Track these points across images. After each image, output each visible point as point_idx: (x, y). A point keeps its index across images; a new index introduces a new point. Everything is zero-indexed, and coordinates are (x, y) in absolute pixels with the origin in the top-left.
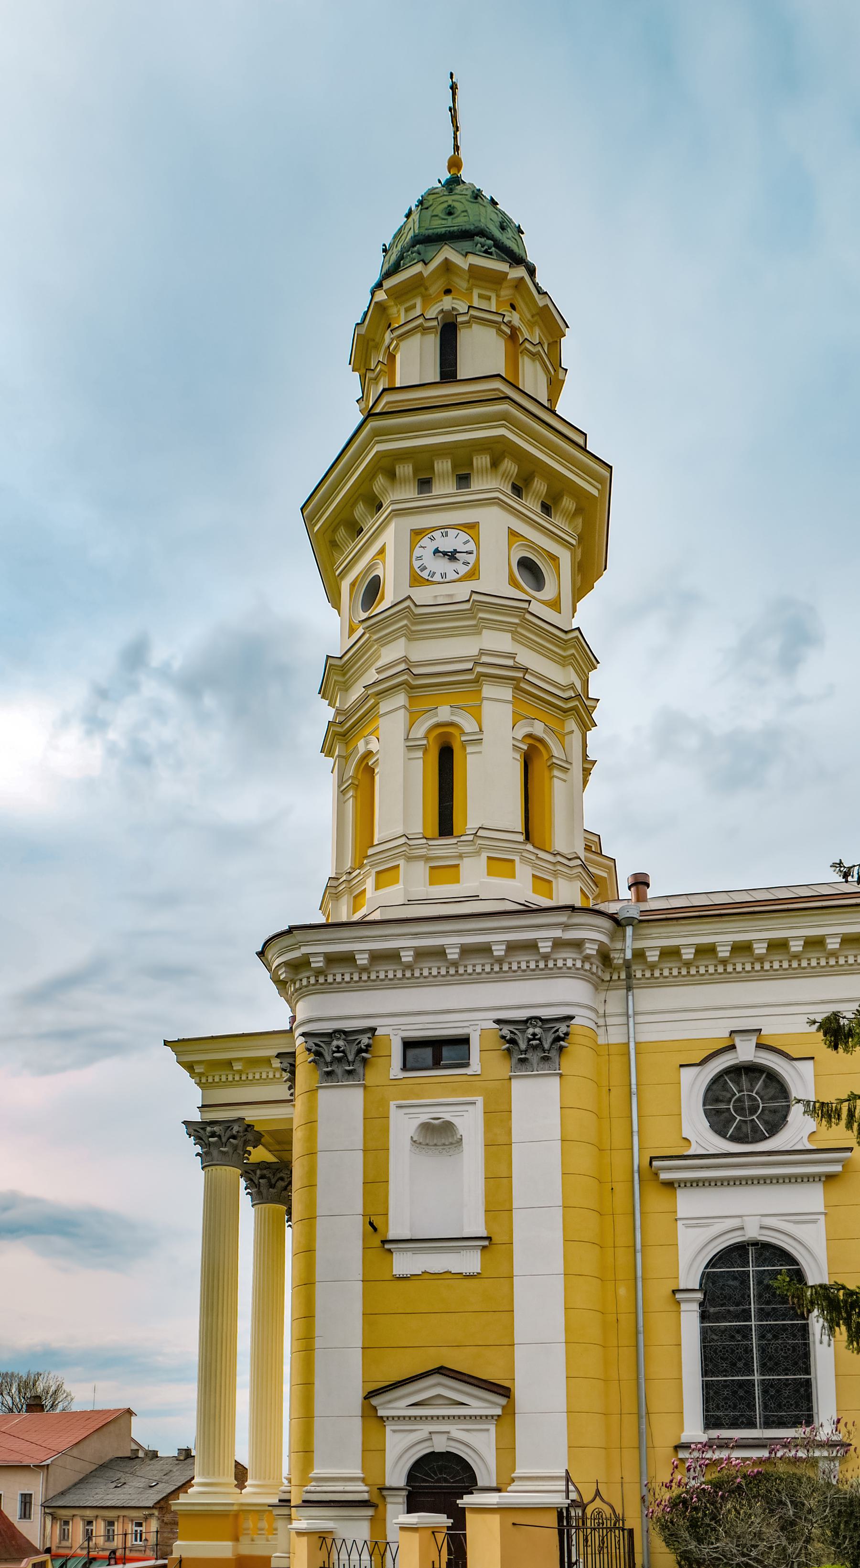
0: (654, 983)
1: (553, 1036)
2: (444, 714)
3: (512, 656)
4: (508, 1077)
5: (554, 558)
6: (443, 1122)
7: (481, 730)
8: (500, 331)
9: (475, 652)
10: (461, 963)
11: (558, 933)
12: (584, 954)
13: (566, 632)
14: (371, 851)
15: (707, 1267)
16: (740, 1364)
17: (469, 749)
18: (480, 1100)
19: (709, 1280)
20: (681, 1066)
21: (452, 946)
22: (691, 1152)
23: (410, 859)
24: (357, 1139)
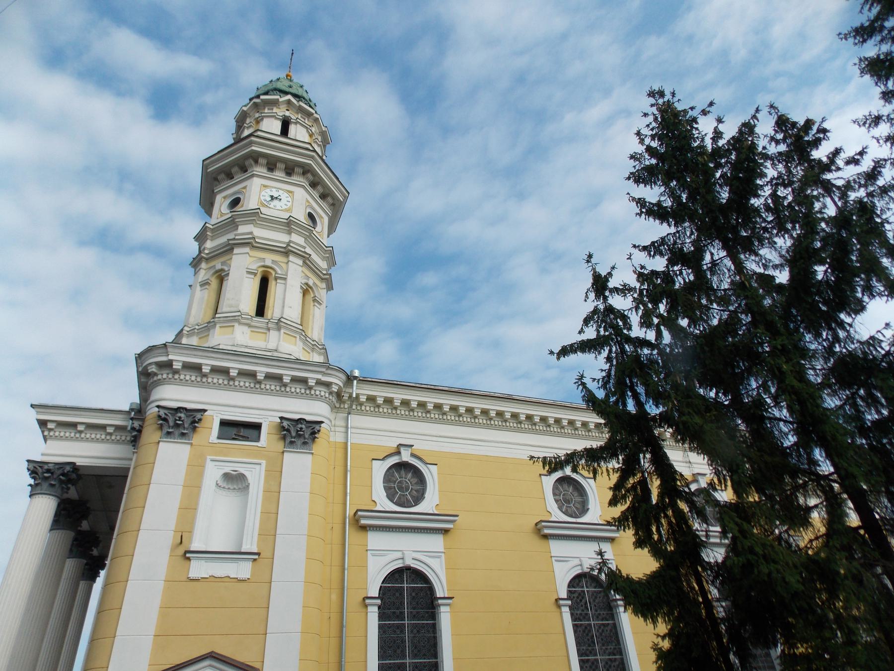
0: (361, 413)
1: (311, 431)
2: (268, 263)
3: (305, 248)
4: (282, 451)
5: (321, 217)
6: (238, 474)
7: (287, 276)
8: (307, 131)
9: (287, 241)
10: (263, 382)
11: (319, 376)
12: (331, 390)
15: (383, 583)
16: (399, 651)
17: (278, 281)
18: (264, 462)
19: (383, 591)
20: (373, 459)
21: (261, 372)
22: (376, 509)
23: (240, 323)
24: (181, 477)
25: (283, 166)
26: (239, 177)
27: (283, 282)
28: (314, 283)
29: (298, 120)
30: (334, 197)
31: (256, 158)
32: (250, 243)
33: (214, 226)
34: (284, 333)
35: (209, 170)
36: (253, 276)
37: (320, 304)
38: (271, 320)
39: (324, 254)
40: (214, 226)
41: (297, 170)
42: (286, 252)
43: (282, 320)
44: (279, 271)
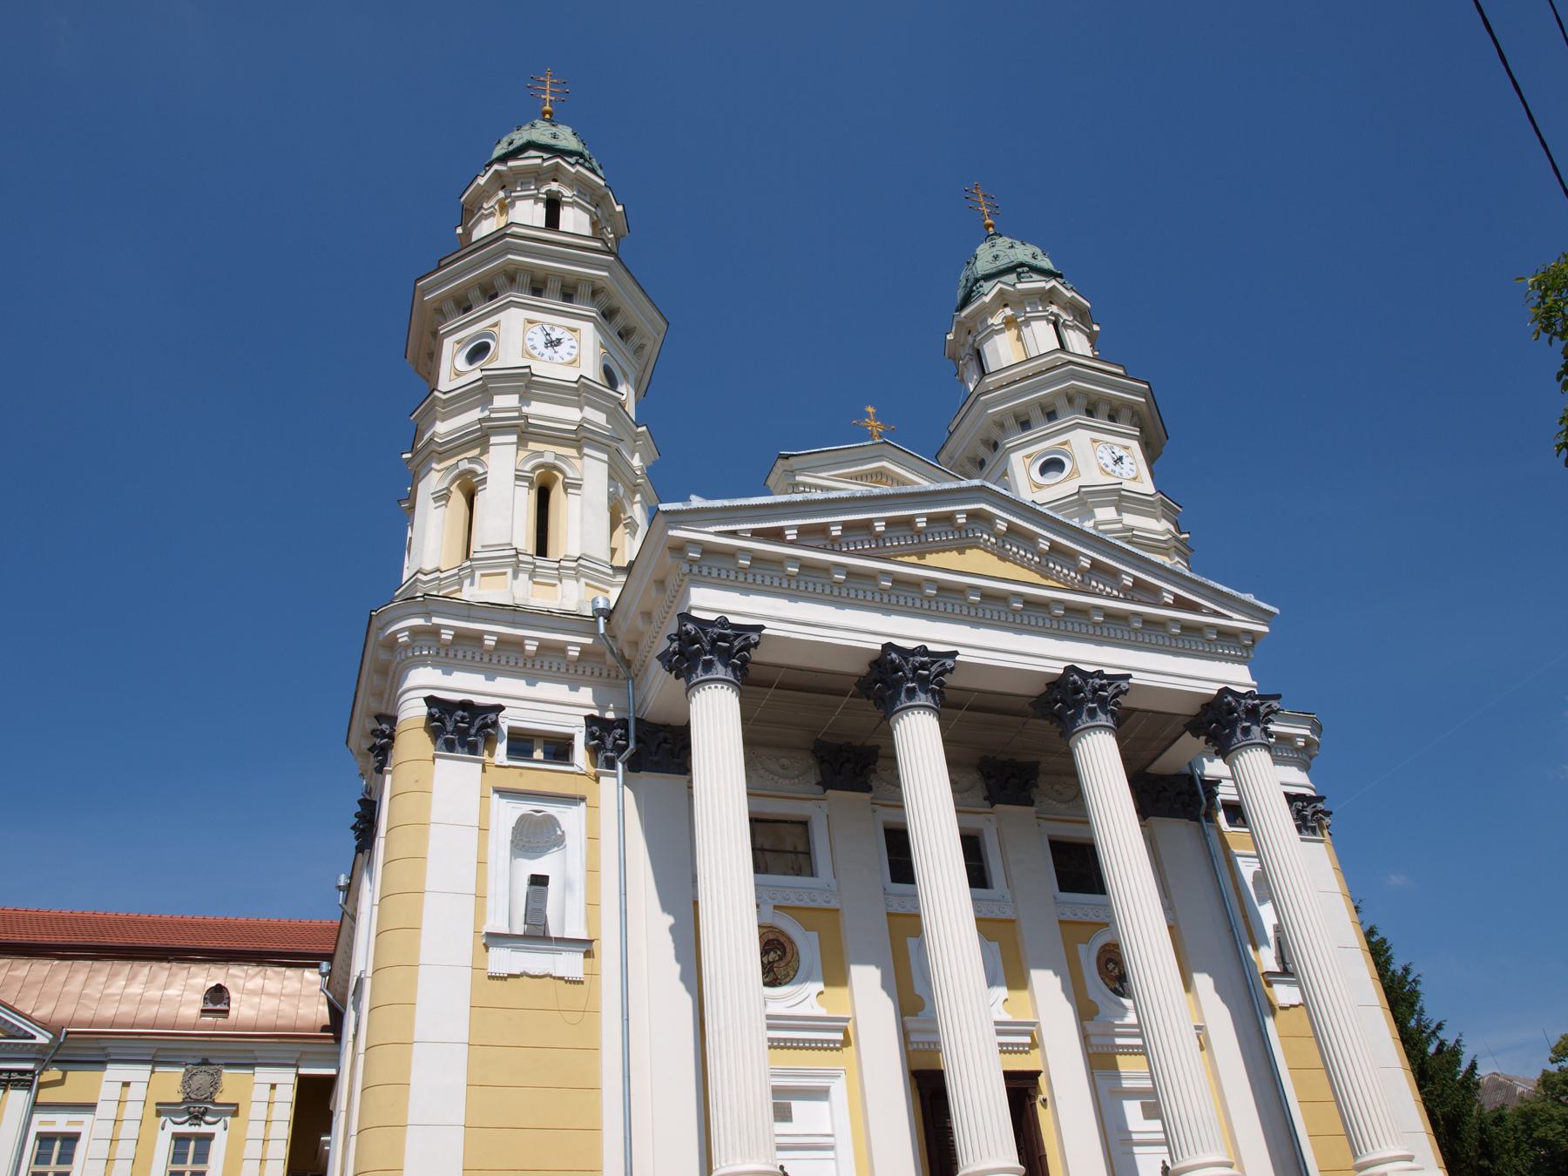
2: (464, 465)
7: (486, 473)
13: (576, 382)
28: (557, 456)
30: (591, 280)
34: (483, 575)
37: (579, 487)
39: (579, 396)
44: (480, 470)
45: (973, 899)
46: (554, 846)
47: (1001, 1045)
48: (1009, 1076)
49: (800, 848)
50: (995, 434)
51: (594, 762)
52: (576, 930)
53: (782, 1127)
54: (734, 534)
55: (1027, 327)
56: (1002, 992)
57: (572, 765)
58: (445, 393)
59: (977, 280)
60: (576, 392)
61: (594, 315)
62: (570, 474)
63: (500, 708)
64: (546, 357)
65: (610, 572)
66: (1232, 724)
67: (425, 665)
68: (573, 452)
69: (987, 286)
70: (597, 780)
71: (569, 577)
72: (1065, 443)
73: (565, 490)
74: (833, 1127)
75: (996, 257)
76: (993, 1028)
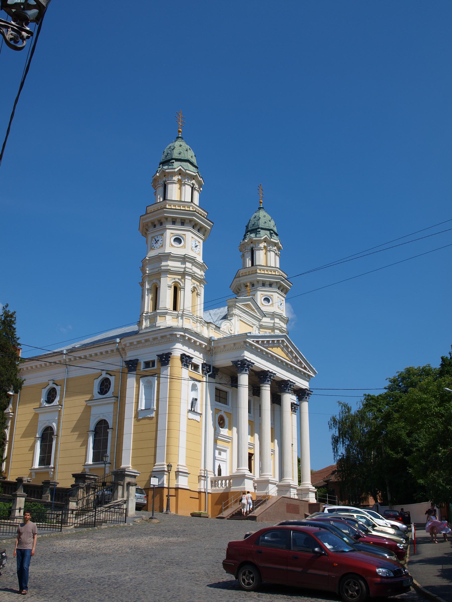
2: (177, 280)
3: (191, 269)
7: (185, 286)
13: (202, 263)
14: (158, 311)
17: (181, 290)
25: (180, 221)
26: (158, 227)
27: (183, 290)
29: (186, 182)
31: (166, 218)
32: (168, 272)
33: (150, 258)
34: (185, 318)
35: (144, 222)
36: (170, 288)
37: (200, 295)
38: (179, 313)
39: (201, 267)
40: (150, 258)
41: (186, 221)
42: (184, 274)
43: (184, 312)
44: (182, 285)
45: (249, 416)
46: (194, 390)
47: (249, 447)
48: (249, 454)
49: (226, 398)
50: (255, 283)
51: (203, 373)
52: (199, 411)
53: (219, 456)
54: (253, 341)
55: (269, 252)
56: (250, 436)
57: (199, 373)
58: (172, 254)
59: (259, 228)
60: (201, 266)
61: (203, 238)
62: (198, 292)
63: (193, 358)
64: (194, 251)
65: (204, 322)
66: (304, 395)
67: (180, 343)
68: (198, 284)
69: (262, 232)
70: (203, 377)
71: (198, 322)
72: (272, 295)
73: (197, 296)
74: (226, 458)
75: (265, 222)
76: (248, 444)
